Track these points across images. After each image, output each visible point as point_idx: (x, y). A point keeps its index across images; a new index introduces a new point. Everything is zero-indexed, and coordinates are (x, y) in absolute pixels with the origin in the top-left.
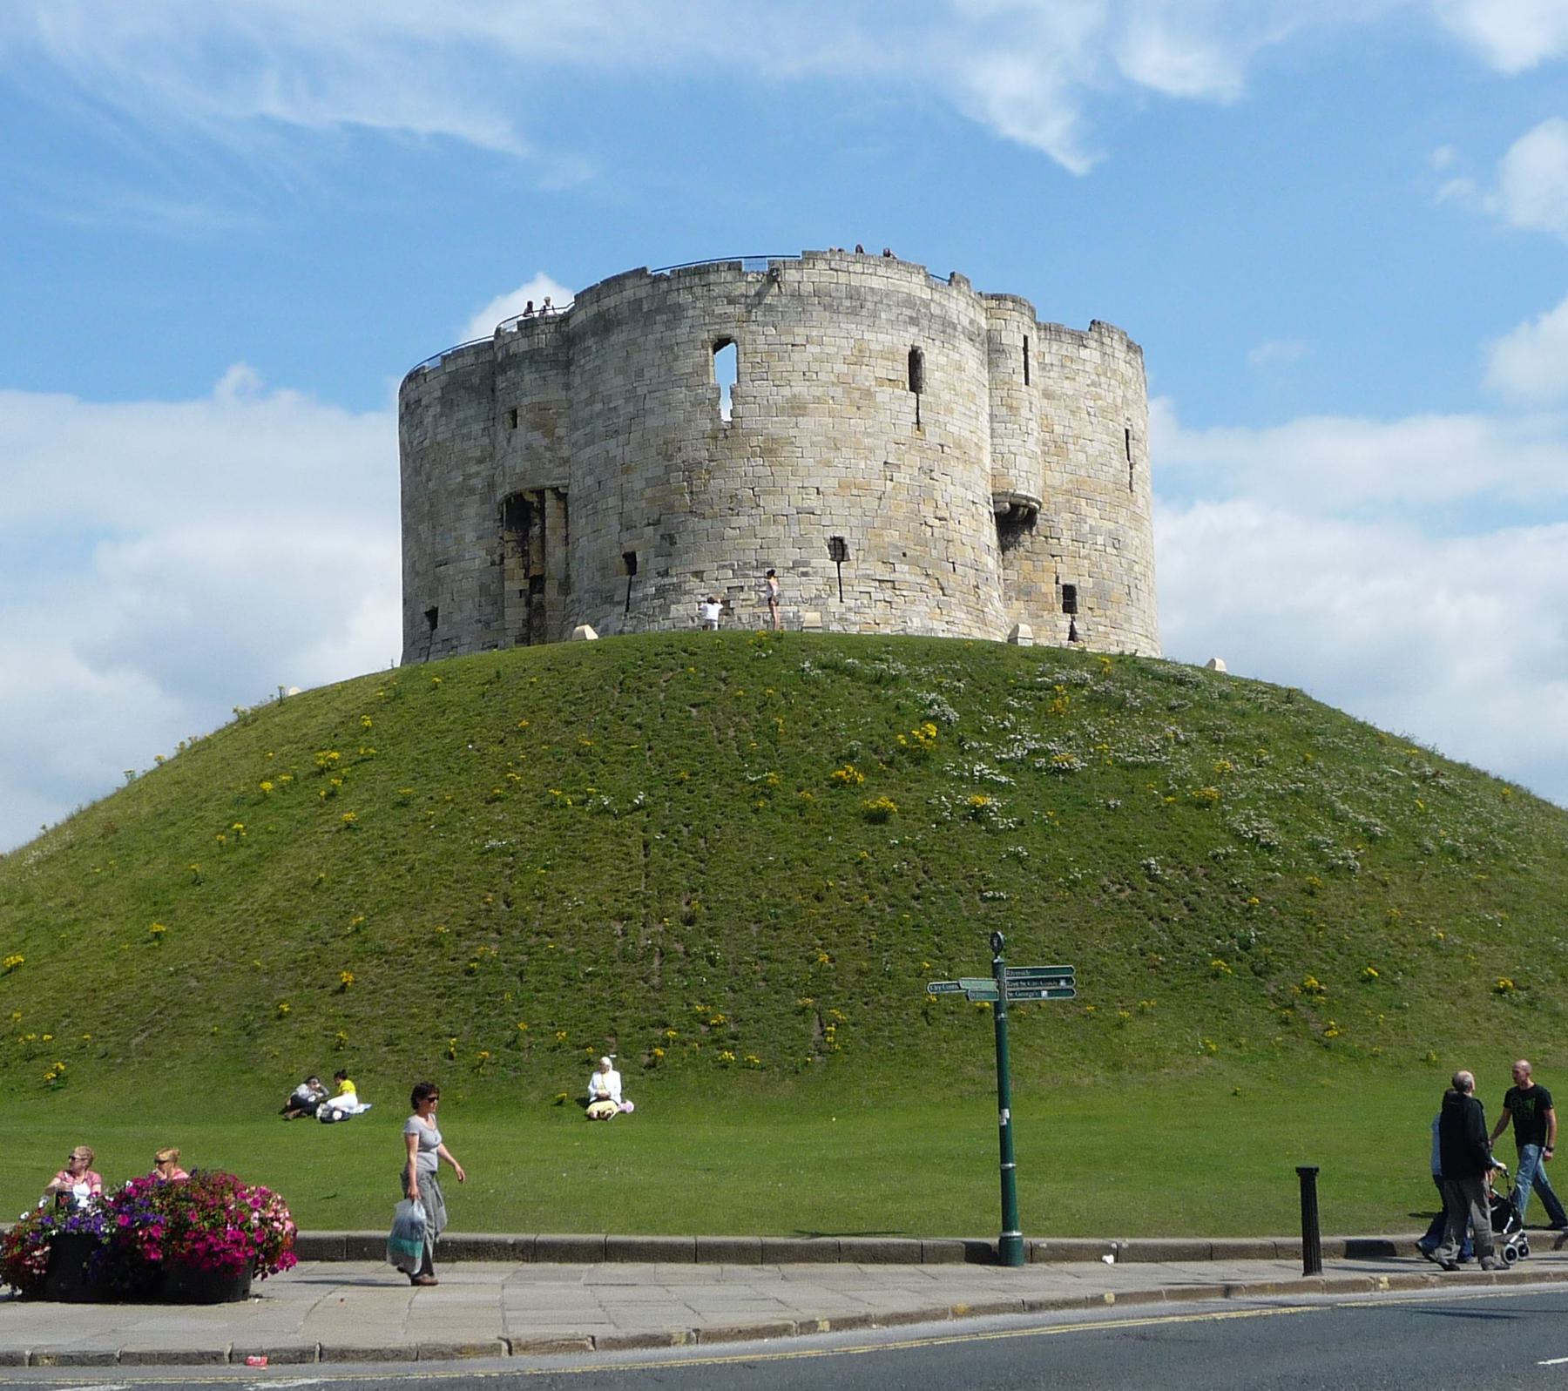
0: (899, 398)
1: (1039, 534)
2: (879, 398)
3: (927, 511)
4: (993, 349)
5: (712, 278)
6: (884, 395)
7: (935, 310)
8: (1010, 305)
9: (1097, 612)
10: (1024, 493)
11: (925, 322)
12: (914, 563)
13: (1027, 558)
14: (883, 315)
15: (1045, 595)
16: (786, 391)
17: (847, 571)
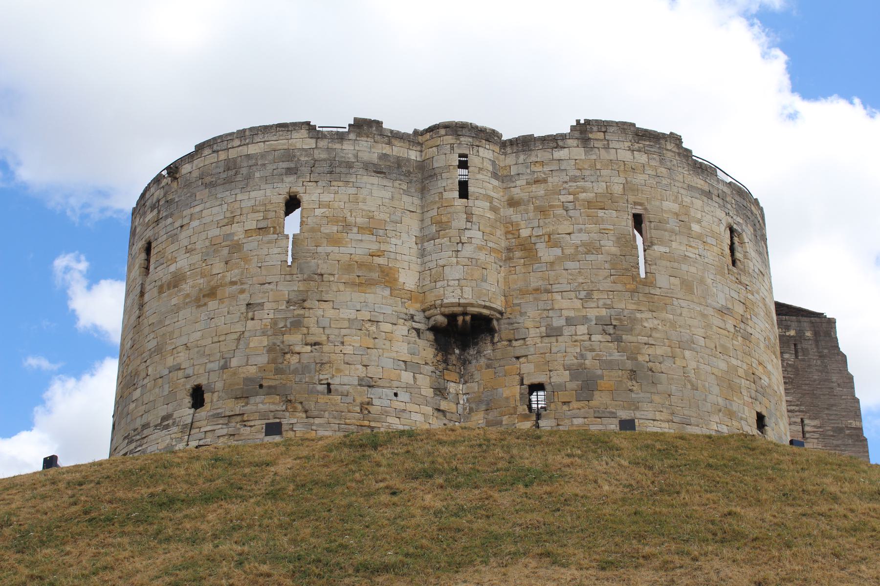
0: (269, 242)
1: (501, 340)
2: (246, 247)
3: (294, 339)
4: (423, 176)
5: (147, 196)
6: (250, 245)
7: (318, 155)
8: (442, 131)
9: (575, 405)
11: (305, 170)
12: (272, 390)
13: (488, 366)
14: (257, 175)
15: (507, 398)
16: (172, 268)
17: (202, 413)
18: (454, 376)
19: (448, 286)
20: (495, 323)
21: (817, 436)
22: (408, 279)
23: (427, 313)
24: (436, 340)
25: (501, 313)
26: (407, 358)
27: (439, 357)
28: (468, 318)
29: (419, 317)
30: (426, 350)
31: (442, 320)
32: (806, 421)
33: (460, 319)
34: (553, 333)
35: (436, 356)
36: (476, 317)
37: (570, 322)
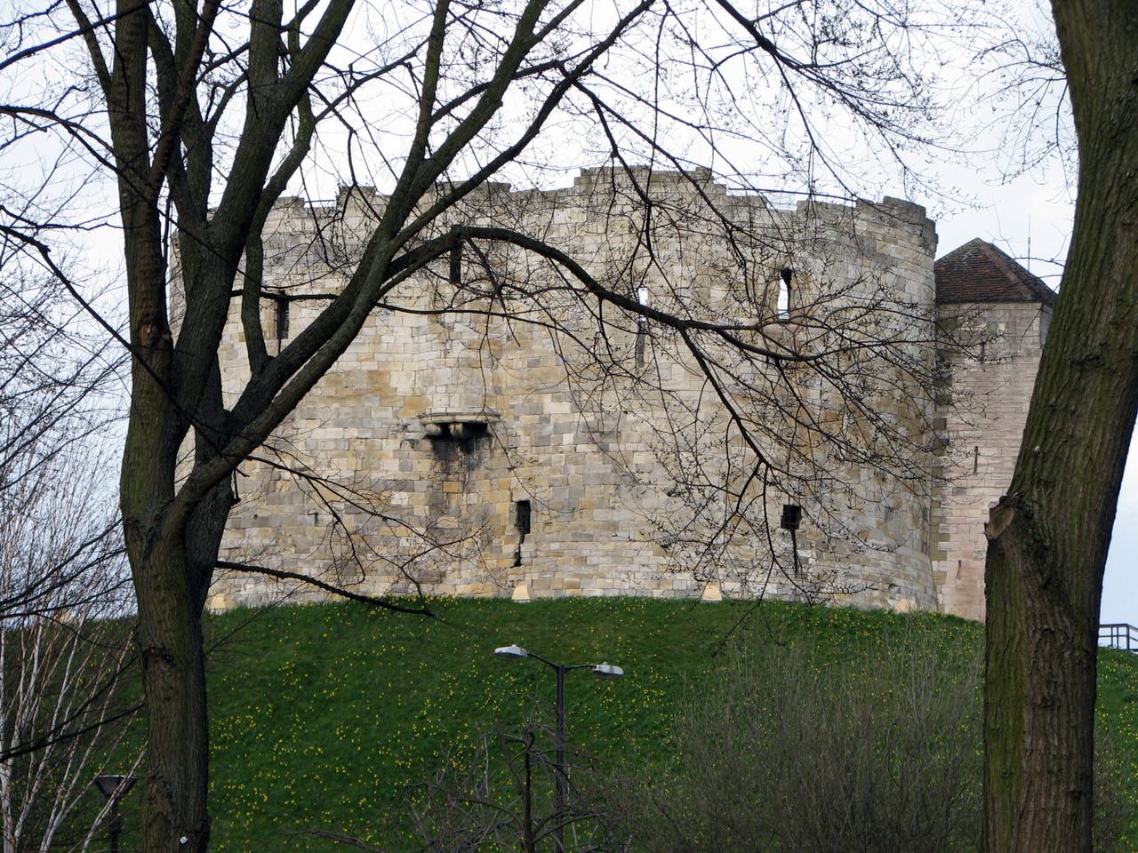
10: (443, 410)
13: (487, 477)
18: (455, 486)
19: (436, 392)
20: (489, 429)
21: (991, 469)
22: (401, 384)
23: (424, 420)
24: (435, 449)
25: (498, 416)
26: (401, 476)
27: (438, 468)
28: (459, 427)
29: (416, 425)
30: (424, 465)
31: (434, 429)
32: (981, 451)
33: (452, 427)
34: (541, 442)
35: (433, 467)
36: (466, 425)
37: (559, 430)
